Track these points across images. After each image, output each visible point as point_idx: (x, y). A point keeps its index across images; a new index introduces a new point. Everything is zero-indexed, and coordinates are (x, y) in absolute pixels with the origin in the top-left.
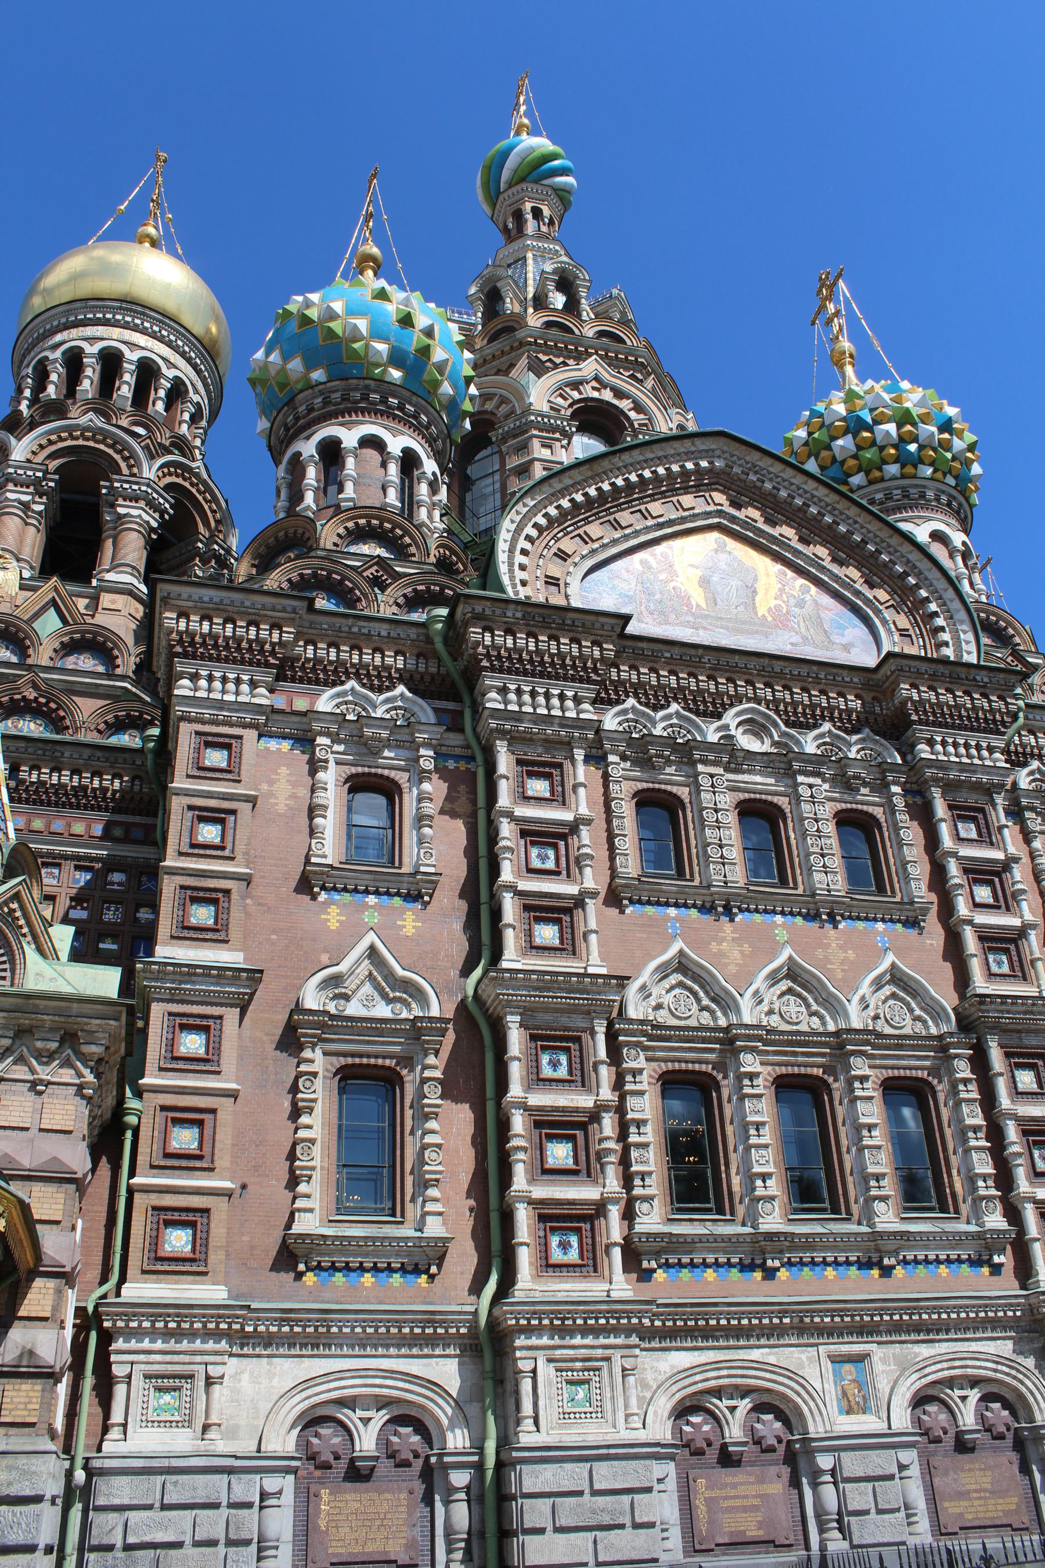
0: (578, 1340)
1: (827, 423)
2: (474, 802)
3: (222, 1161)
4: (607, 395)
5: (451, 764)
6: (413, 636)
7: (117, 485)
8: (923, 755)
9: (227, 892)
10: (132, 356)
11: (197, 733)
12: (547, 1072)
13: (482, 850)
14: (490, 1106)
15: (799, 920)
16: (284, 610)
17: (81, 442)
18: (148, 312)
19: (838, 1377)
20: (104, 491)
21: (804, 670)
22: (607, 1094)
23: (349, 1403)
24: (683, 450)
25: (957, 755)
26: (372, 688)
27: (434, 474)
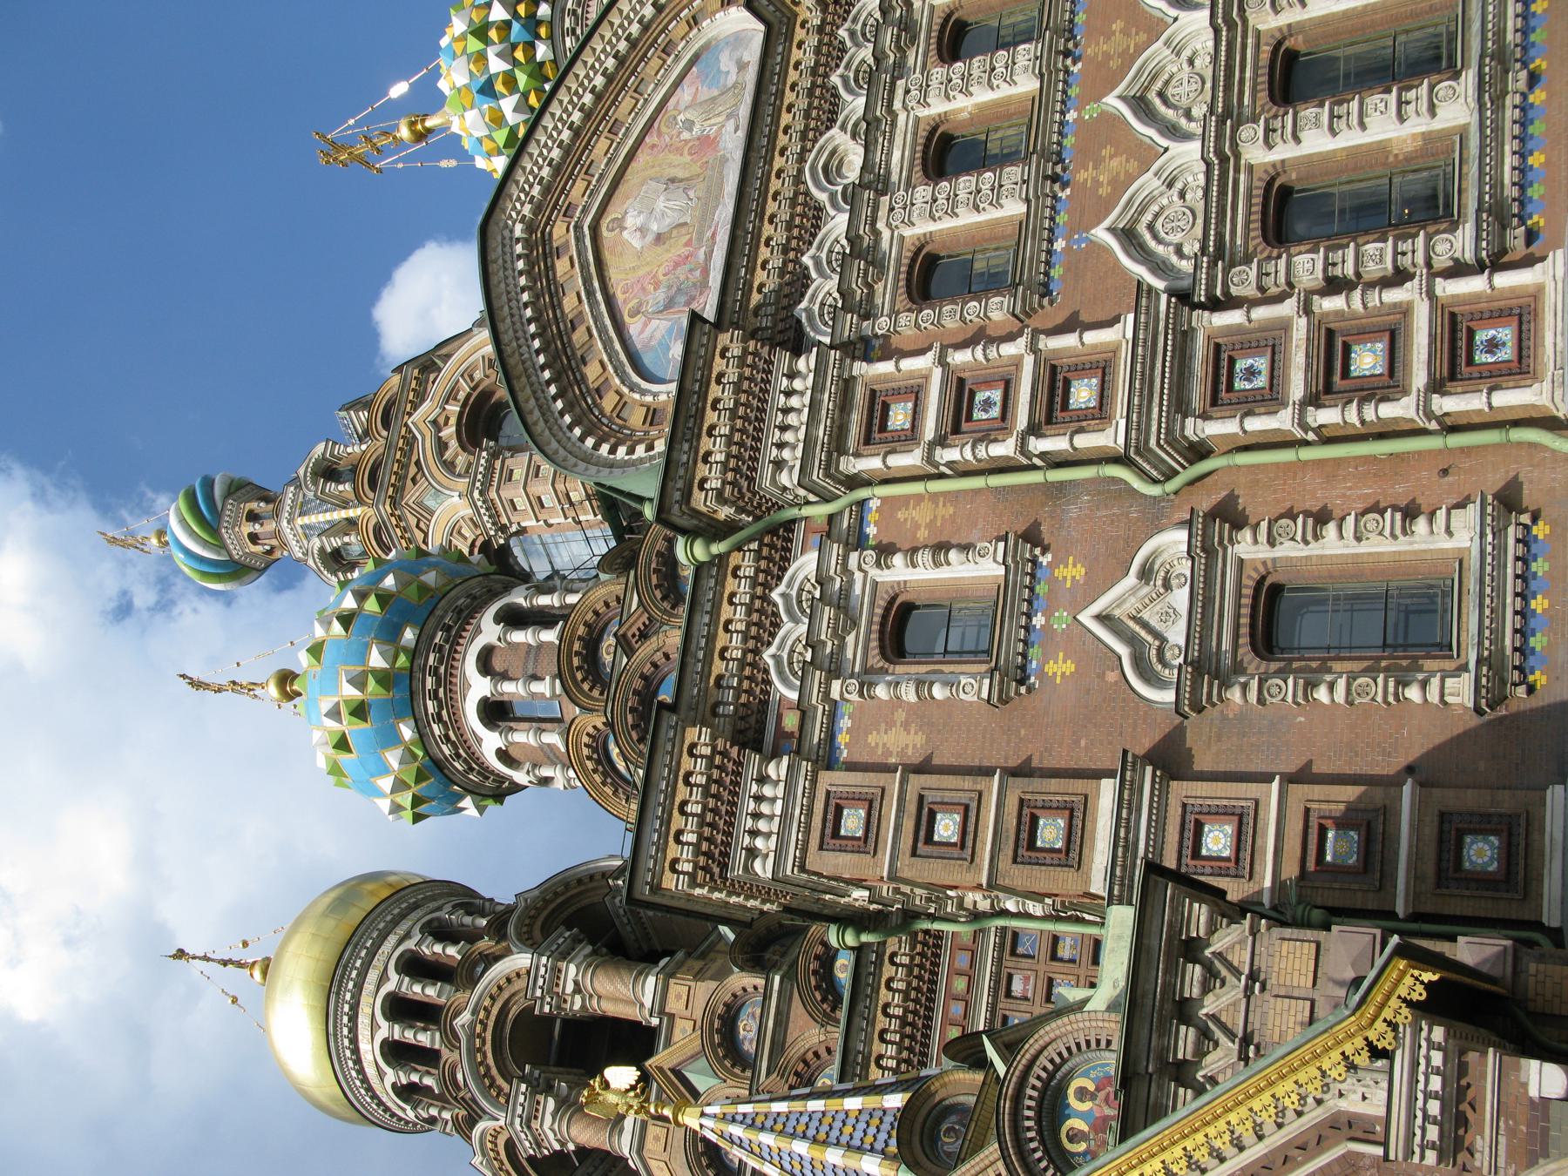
1: (487, 133)
2: (919, 498)
4: (454, 408)
6: (712, 582)
9: (1022, 801)
11: (821, 848)
15: (1073, 92)
16: (673, 740)
17: (489, 1035)
18: (344, 961)
20: (547, 1009)
22: (1288, 308)
24: (501, 273)
26: (773, 635)
27: (527, 589)
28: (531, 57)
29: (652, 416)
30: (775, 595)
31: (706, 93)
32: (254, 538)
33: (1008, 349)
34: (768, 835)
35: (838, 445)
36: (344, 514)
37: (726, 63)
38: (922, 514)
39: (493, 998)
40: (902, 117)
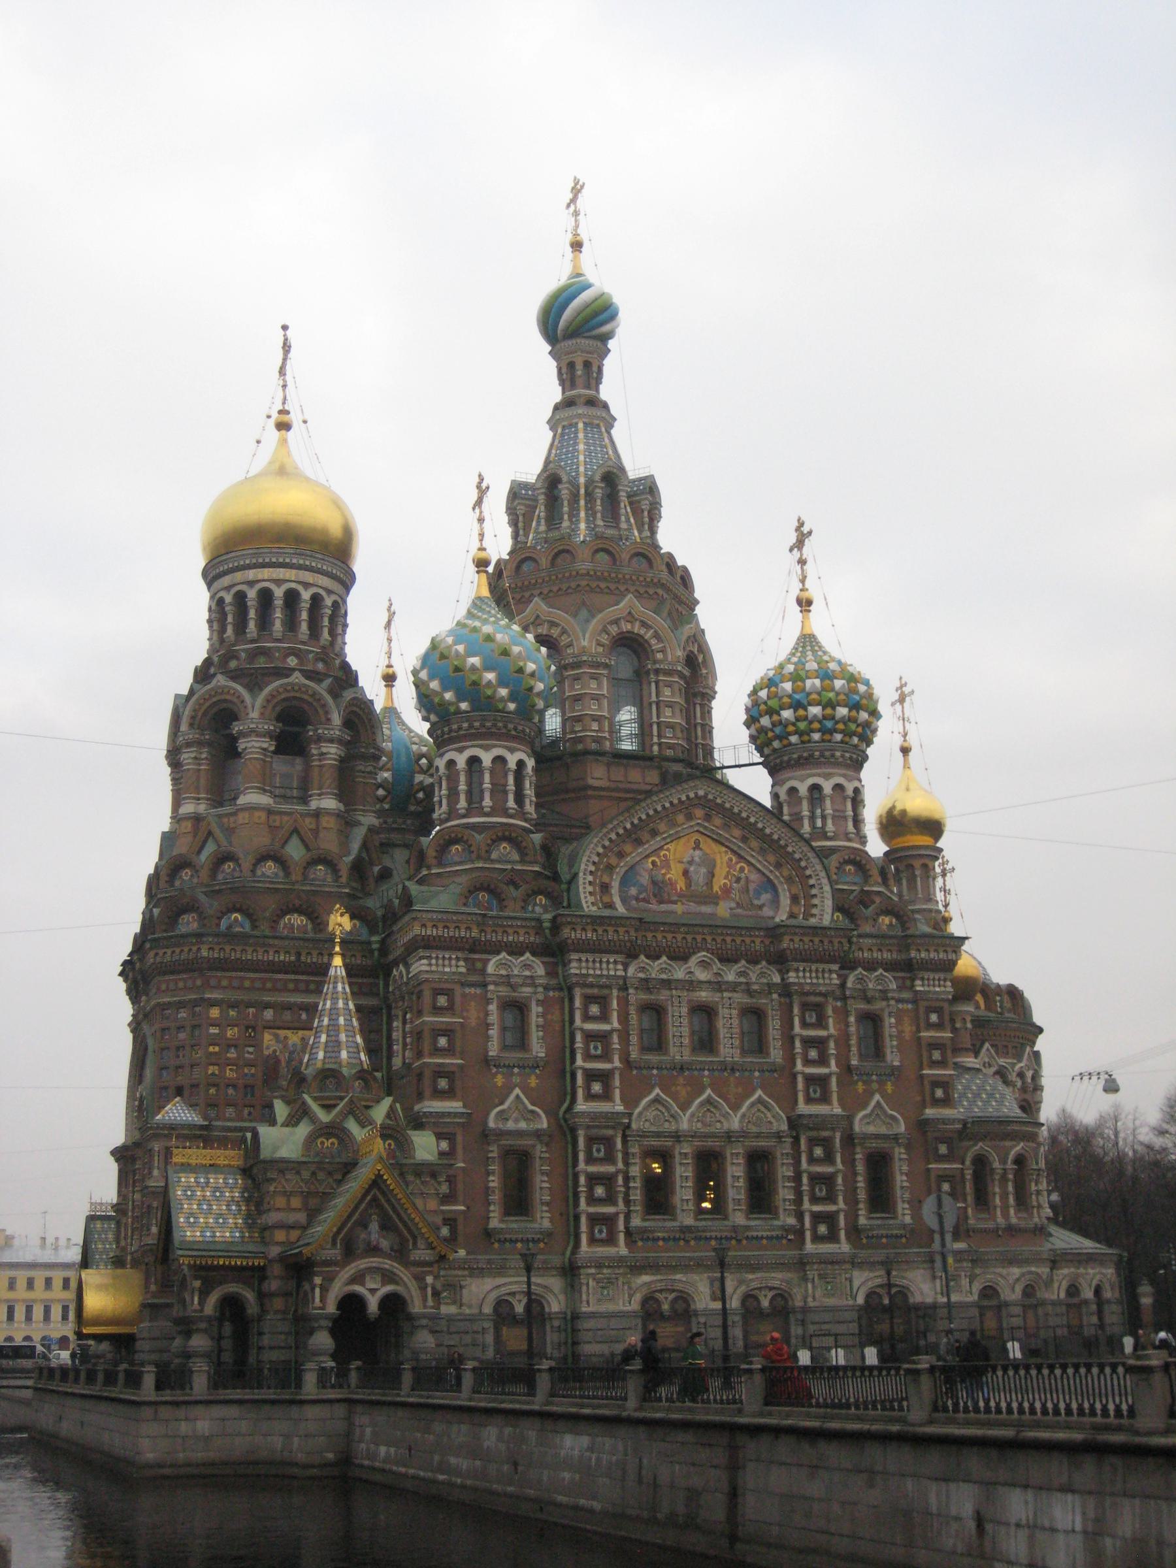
0: (605, 1271)
3: (461, 1199)
4: (637, 628)
5: (551, 994)
7: (320, 731)
8: (791, 980)
9: (453, 1073)
10: (306, 595)
11: (434, 990)
12: (595, 1154)
13: (568, 1044)
14: (570, 1170)
15: (716, 1073)
17: (292, 694)
19: (712, 1285)
21: (734, 931)
22: (620, 1165)
23: (513, 1294)
25: (811, 978)
28: (813, 731)
29: (605, 888)
30: (528, 955)
31: (752, 887)
32: (571, 365)
33: (616, 1058)
34: (437, 965)
35: (585, 985)
36: (582, 491)
37: (766, 897)
38: (556, 1016)
39: (312, 696)
40: (719, 995)
